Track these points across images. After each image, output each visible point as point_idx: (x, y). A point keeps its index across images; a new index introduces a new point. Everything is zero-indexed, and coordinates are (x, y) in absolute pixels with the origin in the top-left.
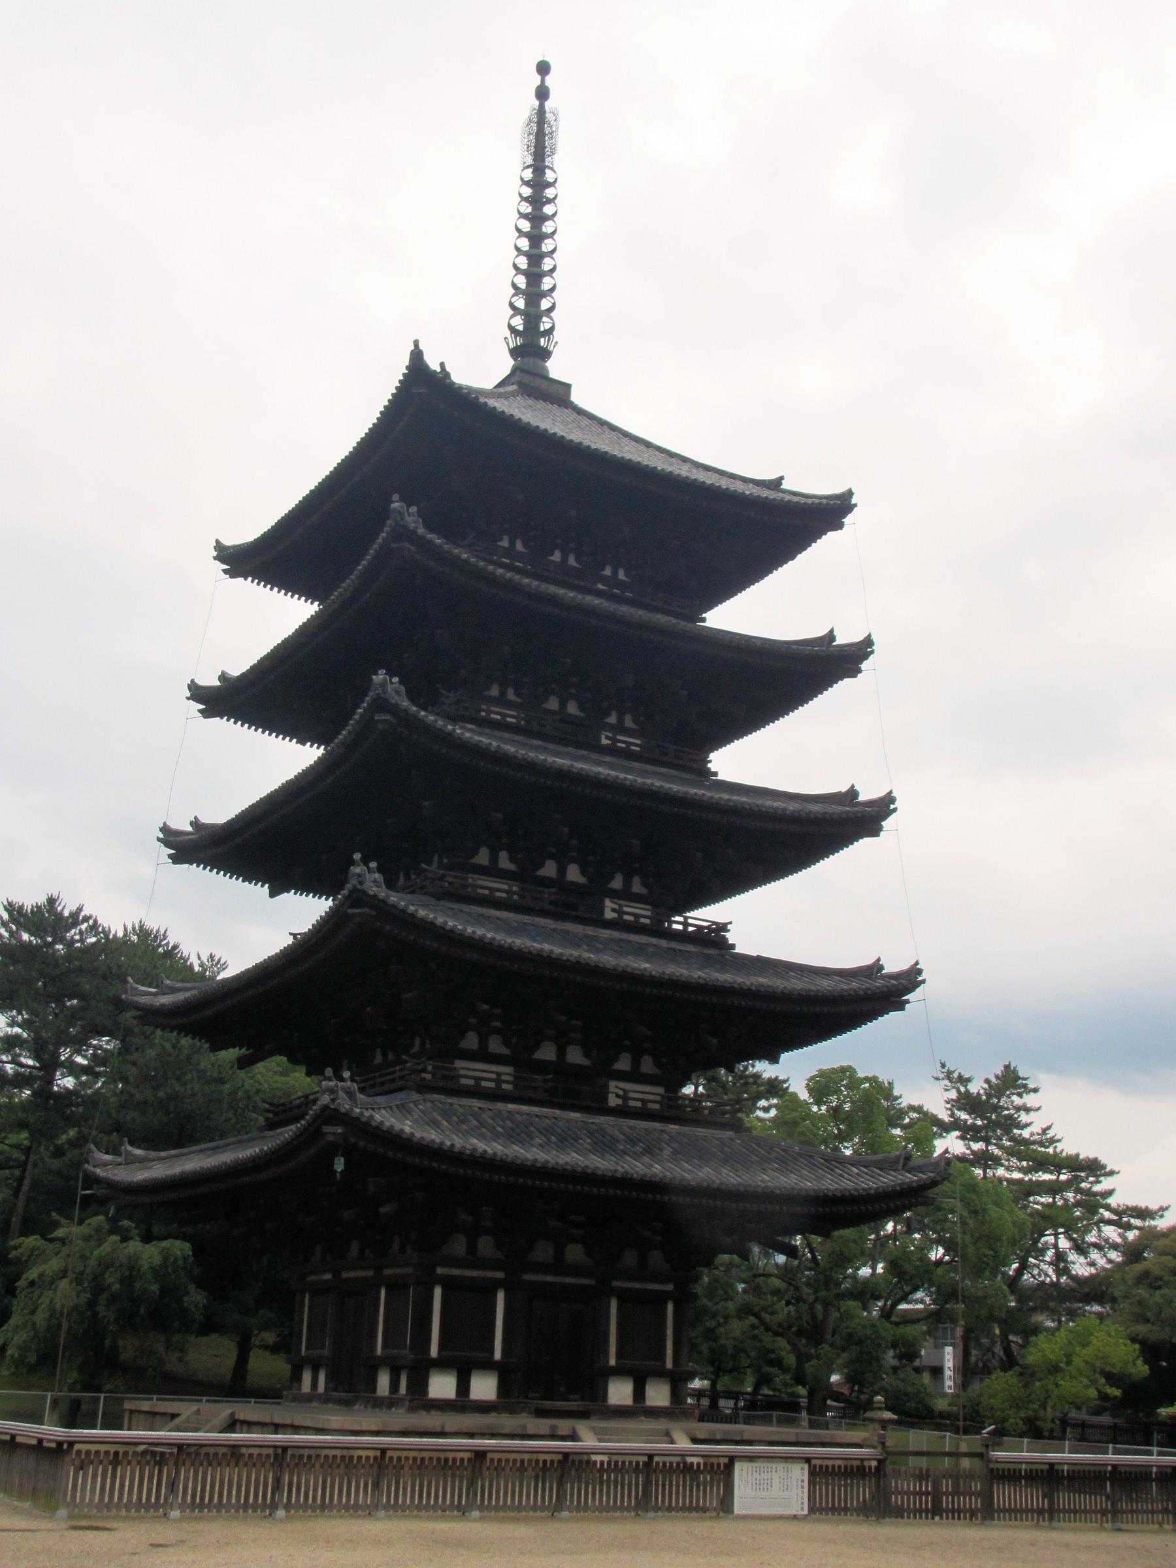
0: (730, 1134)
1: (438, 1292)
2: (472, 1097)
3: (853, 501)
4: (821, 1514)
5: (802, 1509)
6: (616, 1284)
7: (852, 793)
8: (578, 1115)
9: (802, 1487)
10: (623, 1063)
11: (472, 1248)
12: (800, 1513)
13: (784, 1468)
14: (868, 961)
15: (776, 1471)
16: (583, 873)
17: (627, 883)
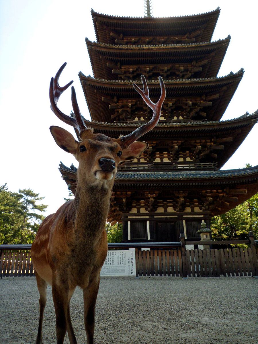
0: (213, 171)
1: (129, 223)
2: (130, 172)
3: (220, 9)
4: (145, 275)
5: (132, 273)
6: (184, 216)
7: (231, 73)
8: (162, 172)
9: (132, 262)
10: (181, 160)
11: (138, 211)
12: (131, 275)
13: (120, 253)
14: (245, 113)
15: (116, 255)
16: (164, 118)
17: (178, 118)
